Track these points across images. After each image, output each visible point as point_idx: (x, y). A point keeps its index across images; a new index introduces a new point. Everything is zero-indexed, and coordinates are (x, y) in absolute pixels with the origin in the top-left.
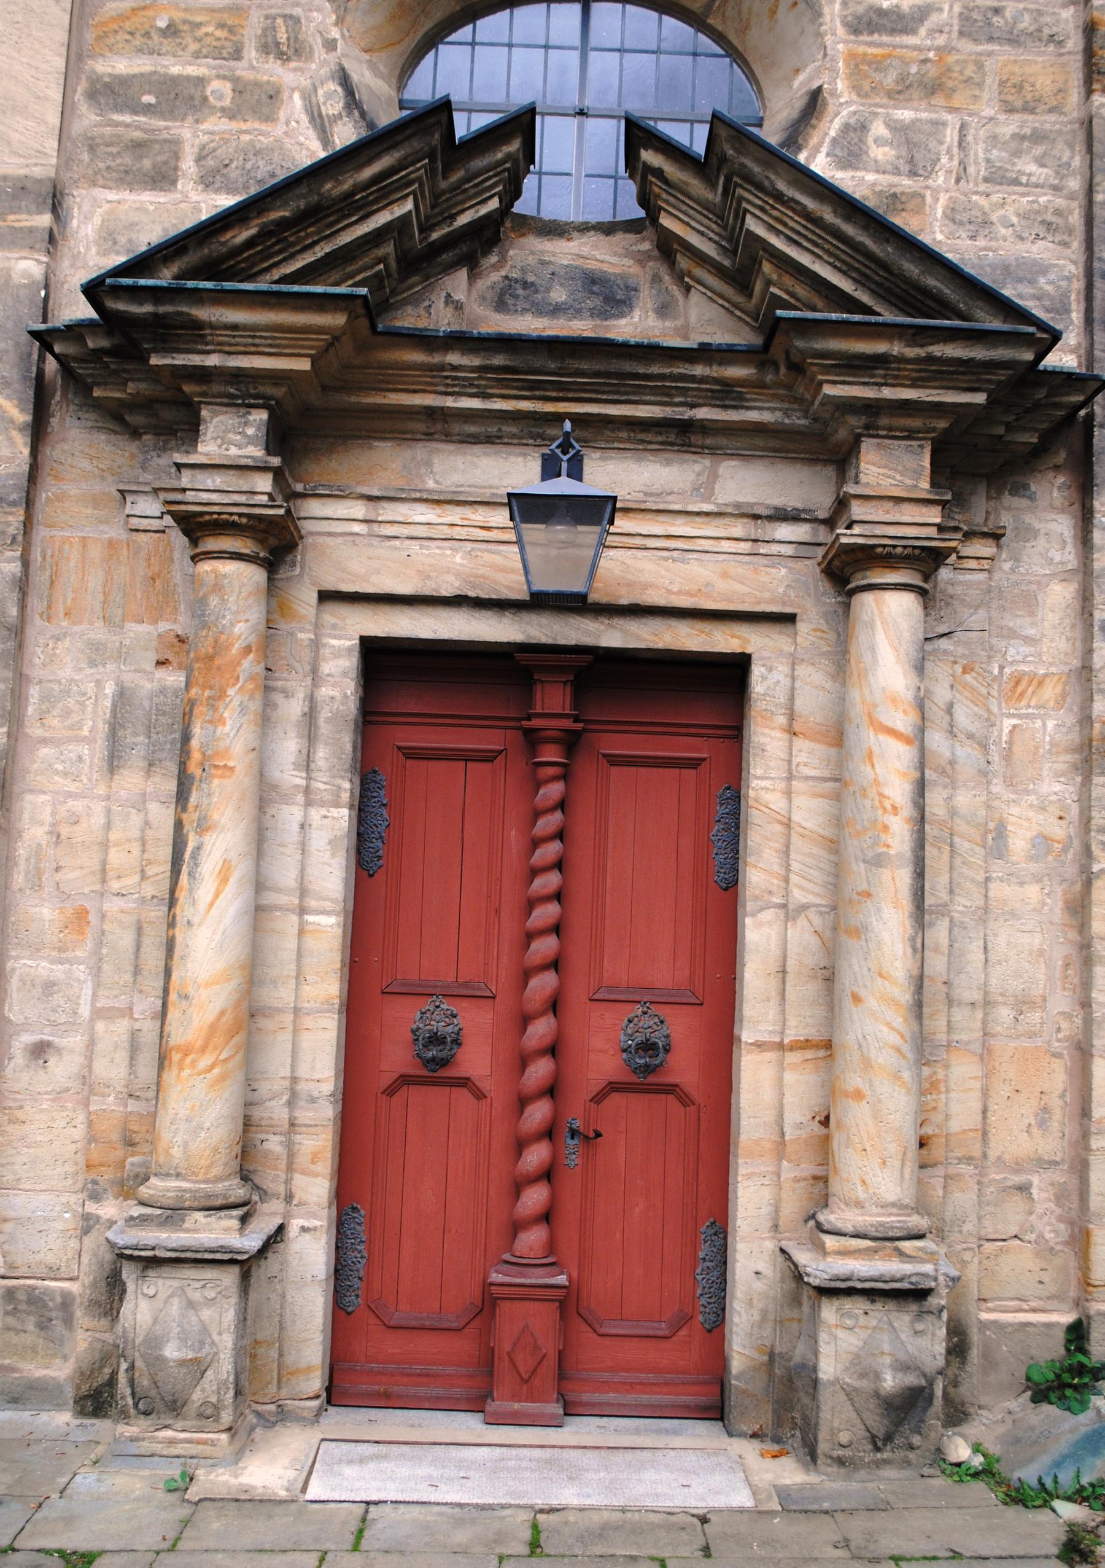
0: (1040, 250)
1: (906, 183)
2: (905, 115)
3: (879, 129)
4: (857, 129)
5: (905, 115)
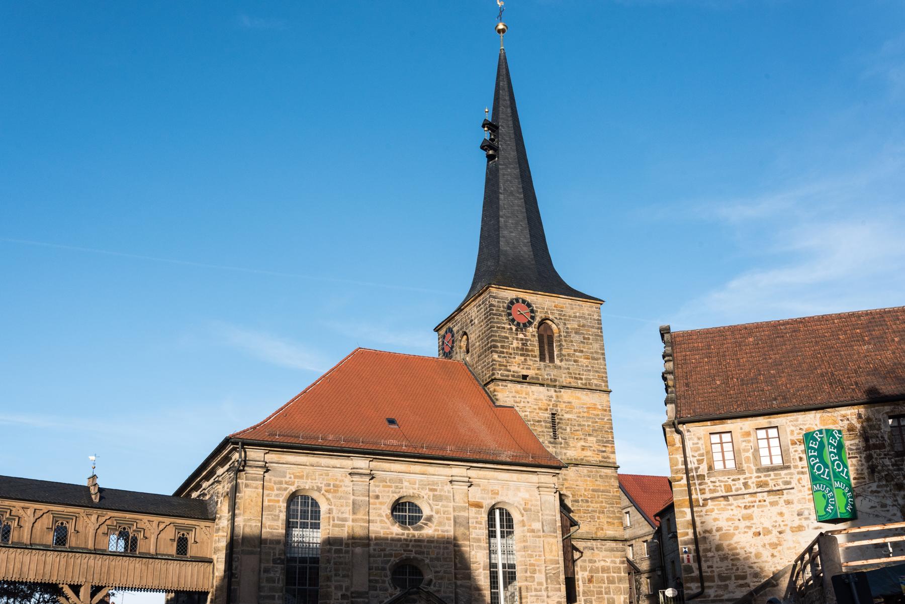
0: (451, 595)
1: (440, 589)
2: (439, 581)
3: (437, 583)
4: (435, 583)
5: (439, 581)
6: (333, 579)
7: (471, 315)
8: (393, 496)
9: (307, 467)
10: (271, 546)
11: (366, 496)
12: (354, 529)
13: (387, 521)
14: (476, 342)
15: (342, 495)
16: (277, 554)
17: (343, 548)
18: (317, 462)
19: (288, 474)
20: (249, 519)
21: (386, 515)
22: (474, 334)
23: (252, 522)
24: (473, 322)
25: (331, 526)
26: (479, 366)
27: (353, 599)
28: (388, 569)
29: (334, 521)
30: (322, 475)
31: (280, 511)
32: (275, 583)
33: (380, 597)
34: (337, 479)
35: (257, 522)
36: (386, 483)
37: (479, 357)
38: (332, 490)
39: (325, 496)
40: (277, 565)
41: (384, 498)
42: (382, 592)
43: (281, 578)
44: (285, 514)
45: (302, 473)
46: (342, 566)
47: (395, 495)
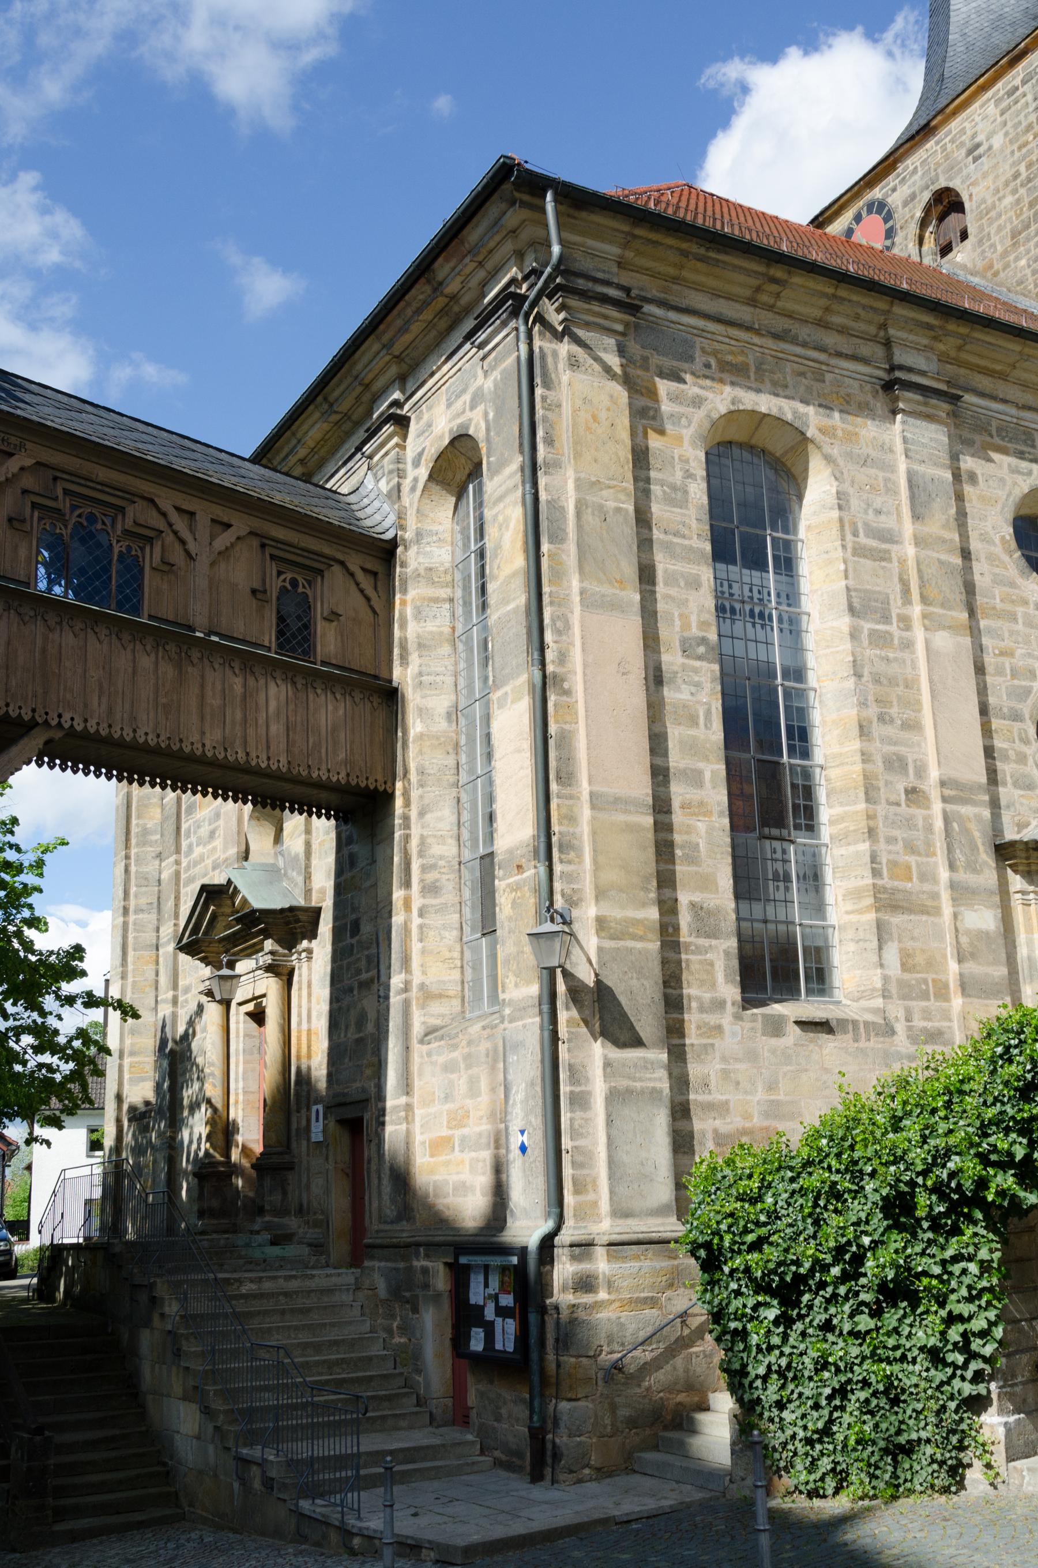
6: (875, 734)
7: (969, 133)
8: (1015, 484)
9: (756, 340)
10: (673, 591)
11: (943, 466)
12: (922, 567)
13: (1006, 558)
14: (999, 199)
15: (873, 454)
16: (694, 625)
17: (893, 628)
18: (787, 331)
19: (698, 353)
20: (593, 484)
21: (1003, 538)
22: (991, 178)
23: (605, 493)
24: (981, 150)
25: (849, 550)
26: (1017, 259)
27: (949, 807)
28: (1027, 716)
29: (855, 534)
30: (802, 374)
31: (689, 475)
32: (697, 724)
33: (1017, 805)
34: (848, 395)
35: (622, 497)
36: (992, 436)
37: (1015, 234)
38: (840, 433)
39: (819, 448)
40: (697, 664)
41: (991, 482)
42: (1022, 793)
43: (714, 710)
44: (704, 485)
45: (740, 359)
46: (900, 690)
47: (1020, 479)
